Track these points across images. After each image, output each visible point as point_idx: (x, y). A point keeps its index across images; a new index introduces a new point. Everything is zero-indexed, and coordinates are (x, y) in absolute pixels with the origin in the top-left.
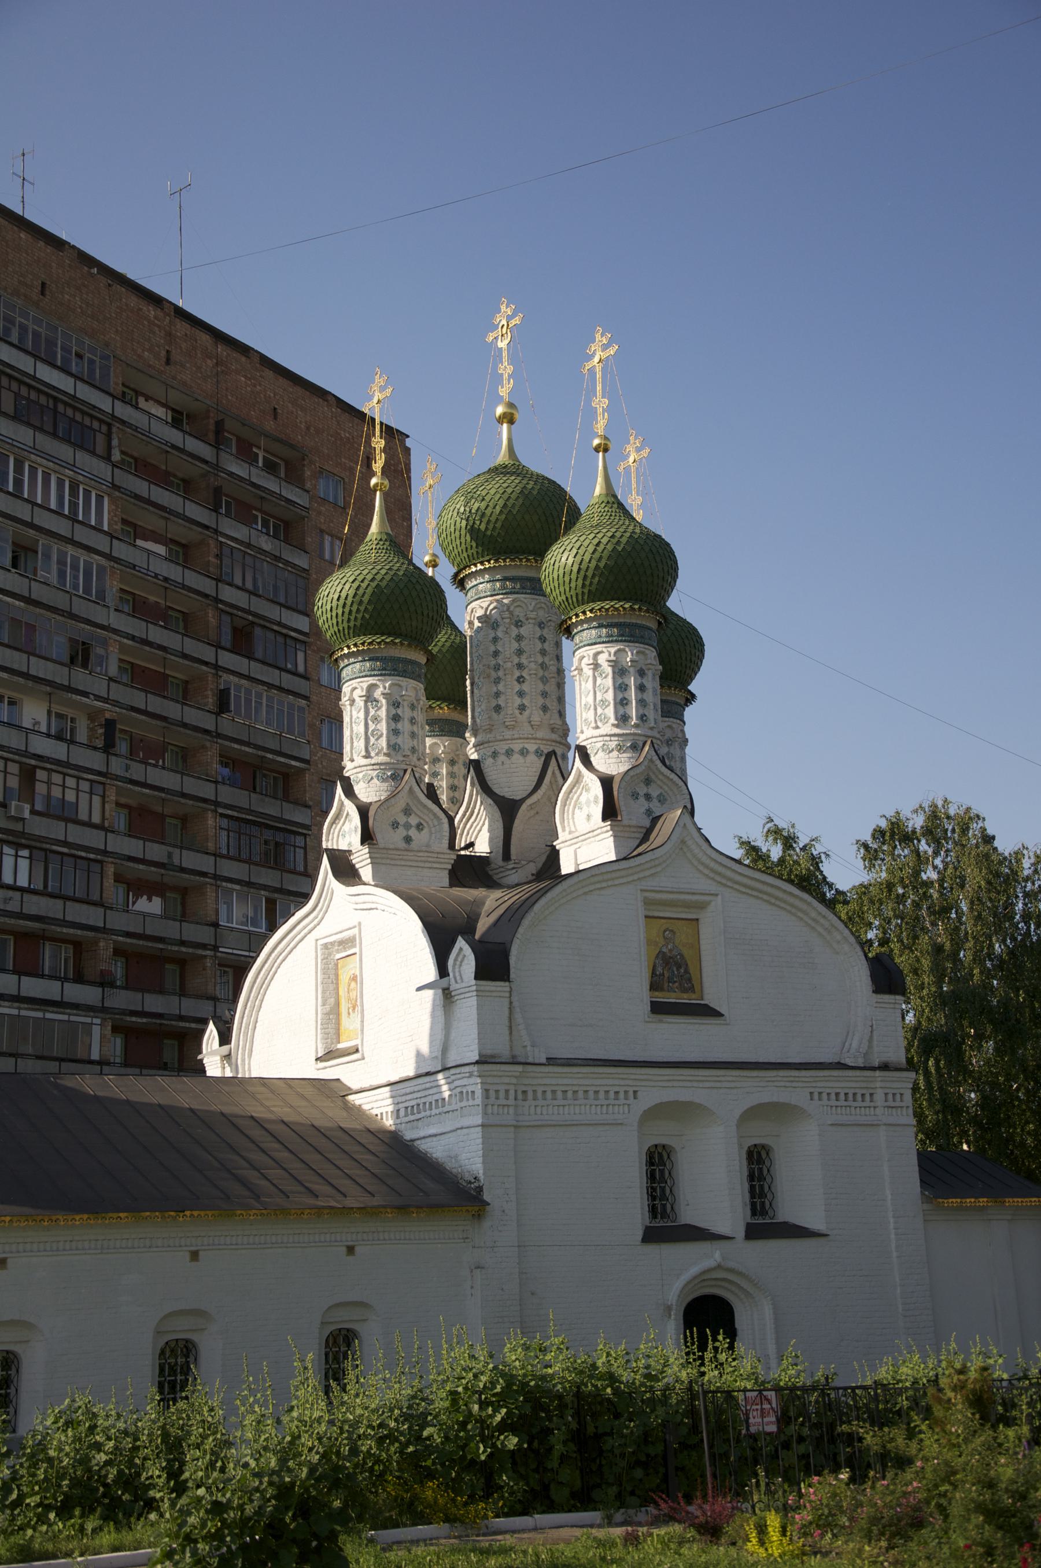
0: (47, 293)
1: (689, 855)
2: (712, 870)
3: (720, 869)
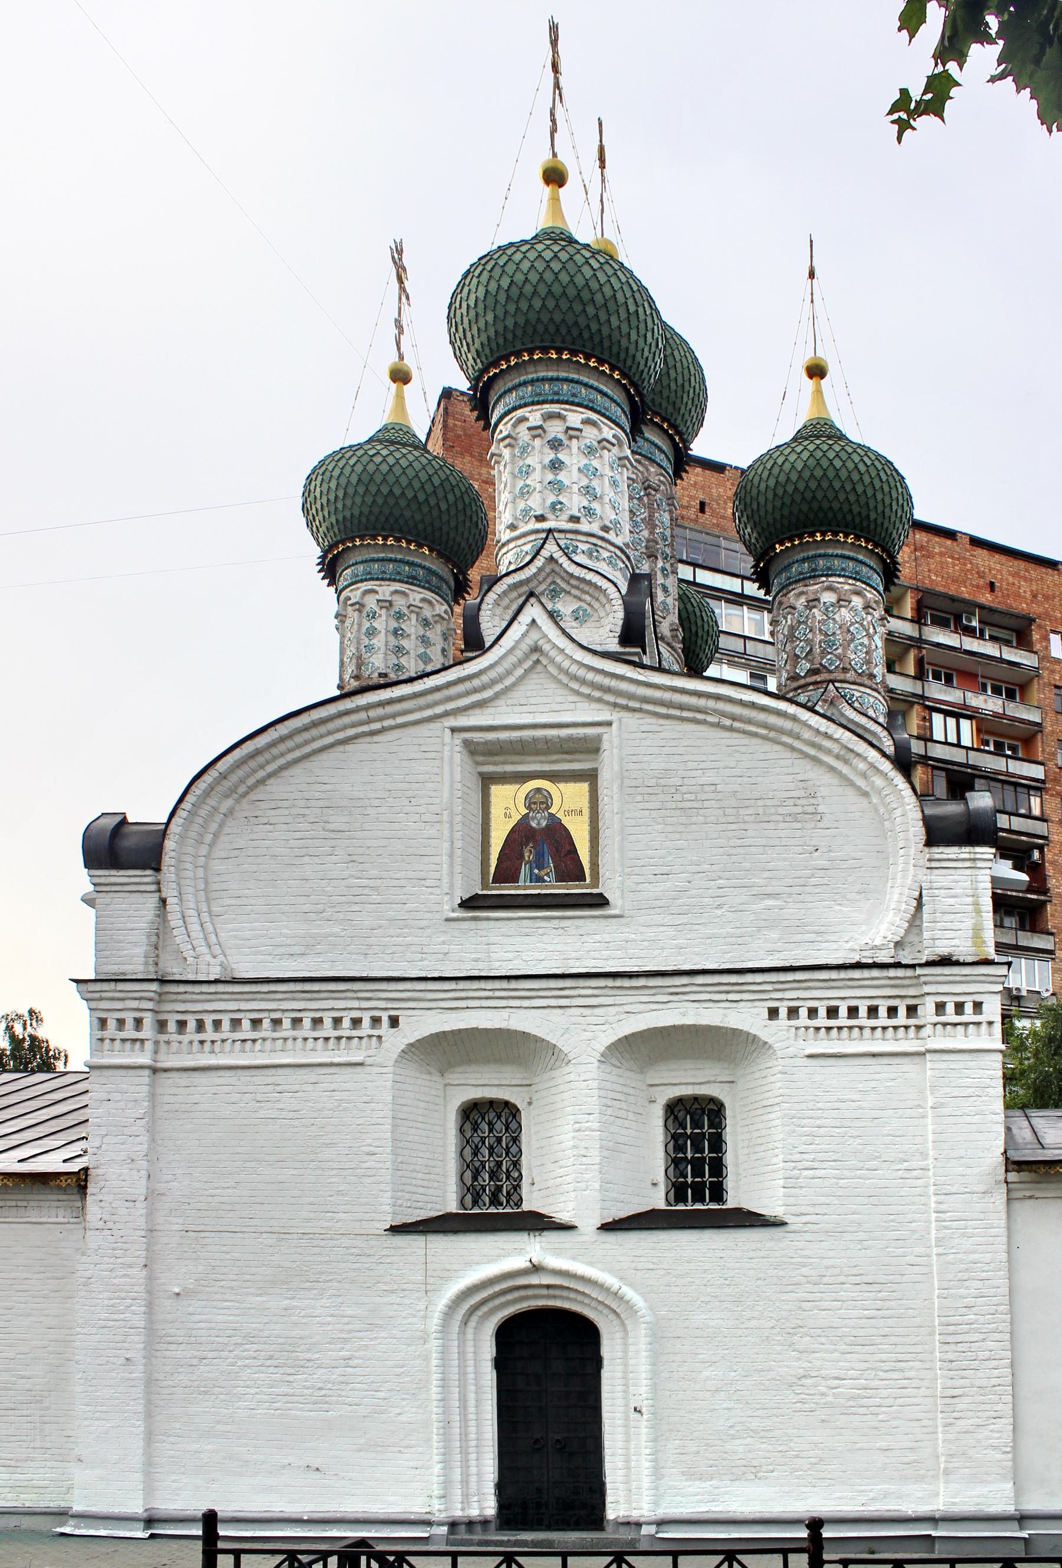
1: (551, 668)
2: (593, 685)
3: (607, 681)
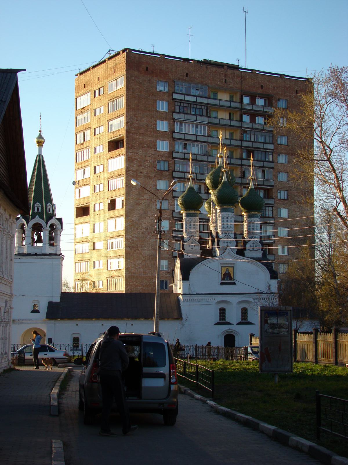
0: (188, 76)
